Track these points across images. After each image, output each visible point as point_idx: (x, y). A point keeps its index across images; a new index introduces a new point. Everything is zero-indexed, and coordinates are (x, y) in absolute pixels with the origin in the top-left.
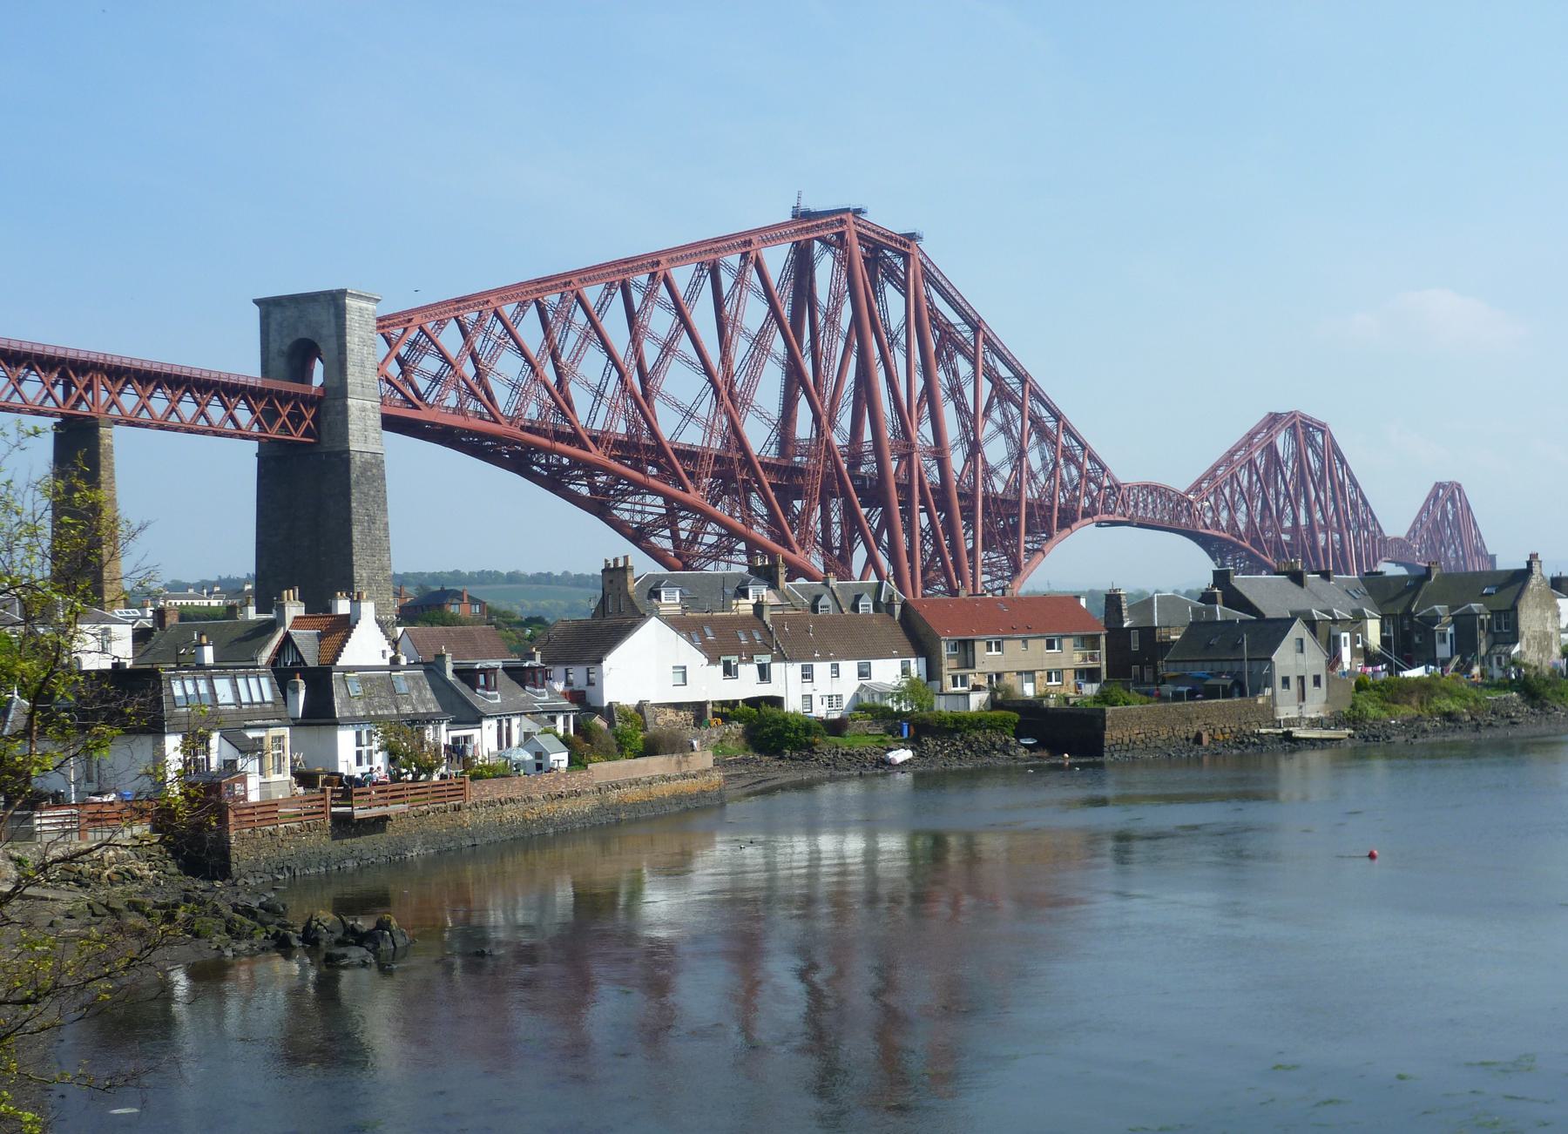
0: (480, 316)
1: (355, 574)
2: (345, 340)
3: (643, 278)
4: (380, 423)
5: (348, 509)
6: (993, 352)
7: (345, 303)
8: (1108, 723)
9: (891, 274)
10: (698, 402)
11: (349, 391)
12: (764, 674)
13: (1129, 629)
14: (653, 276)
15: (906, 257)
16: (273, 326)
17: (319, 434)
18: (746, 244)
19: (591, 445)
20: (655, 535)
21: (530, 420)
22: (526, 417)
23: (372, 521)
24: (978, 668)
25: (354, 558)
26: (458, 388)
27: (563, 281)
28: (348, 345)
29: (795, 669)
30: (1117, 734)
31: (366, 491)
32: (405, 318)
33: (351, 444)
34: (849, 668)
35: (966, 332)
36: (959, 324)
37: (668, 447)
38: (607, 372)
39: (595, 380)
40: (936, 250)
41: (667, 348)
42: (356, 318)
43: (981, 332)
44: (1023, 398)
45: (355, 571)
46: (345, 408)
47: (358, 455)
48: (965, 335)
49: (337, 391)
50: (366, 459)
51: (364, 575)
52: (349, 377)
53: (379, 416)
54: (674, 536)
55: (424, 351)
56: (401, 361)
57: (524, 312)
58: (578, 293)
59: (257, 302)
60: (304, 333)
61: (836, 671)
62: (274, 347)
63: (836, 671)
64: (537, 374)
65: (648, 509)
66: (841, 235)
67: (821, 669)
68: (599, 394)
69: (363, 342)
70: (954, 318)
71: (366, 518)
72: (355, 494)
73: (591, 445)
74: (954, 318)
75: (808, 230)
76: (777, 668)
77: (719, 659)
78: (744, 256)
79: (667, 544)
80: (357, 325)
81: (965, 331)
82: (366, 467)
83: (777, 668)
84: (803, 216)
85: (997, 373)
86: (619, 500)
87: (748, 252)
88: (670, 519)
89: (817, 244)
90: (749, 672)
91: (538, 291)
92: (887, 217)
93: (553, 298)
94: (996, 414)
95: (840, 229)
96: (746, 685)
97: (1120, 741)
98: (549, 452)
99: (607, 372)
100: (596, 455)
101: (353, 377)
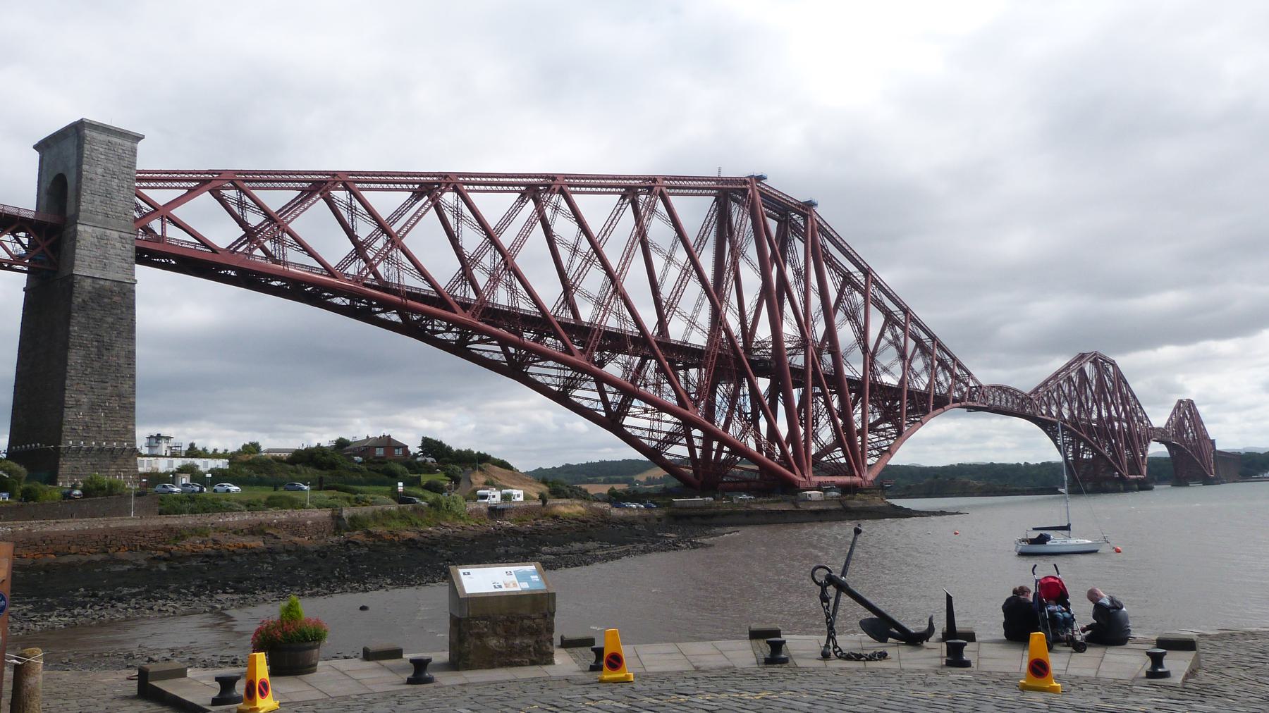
1: (66, 399)
4: (133, 254)
5: (68, 333)
6: (879, 289)
23: (104, 347)
25: (68, 382)
31: (98, 316)
36: (855, 272)
37: (554, 320)
42: (101, 149)
43: (870, 276)
44: (906, 323)
45: (67, 395)
47: (89, 281)
70: (852, 268)
71: (95, 343)
72: (78, 318)
74: (852, 268)
80: (103, 157)
85: (883, 304)
94: (888, 334)
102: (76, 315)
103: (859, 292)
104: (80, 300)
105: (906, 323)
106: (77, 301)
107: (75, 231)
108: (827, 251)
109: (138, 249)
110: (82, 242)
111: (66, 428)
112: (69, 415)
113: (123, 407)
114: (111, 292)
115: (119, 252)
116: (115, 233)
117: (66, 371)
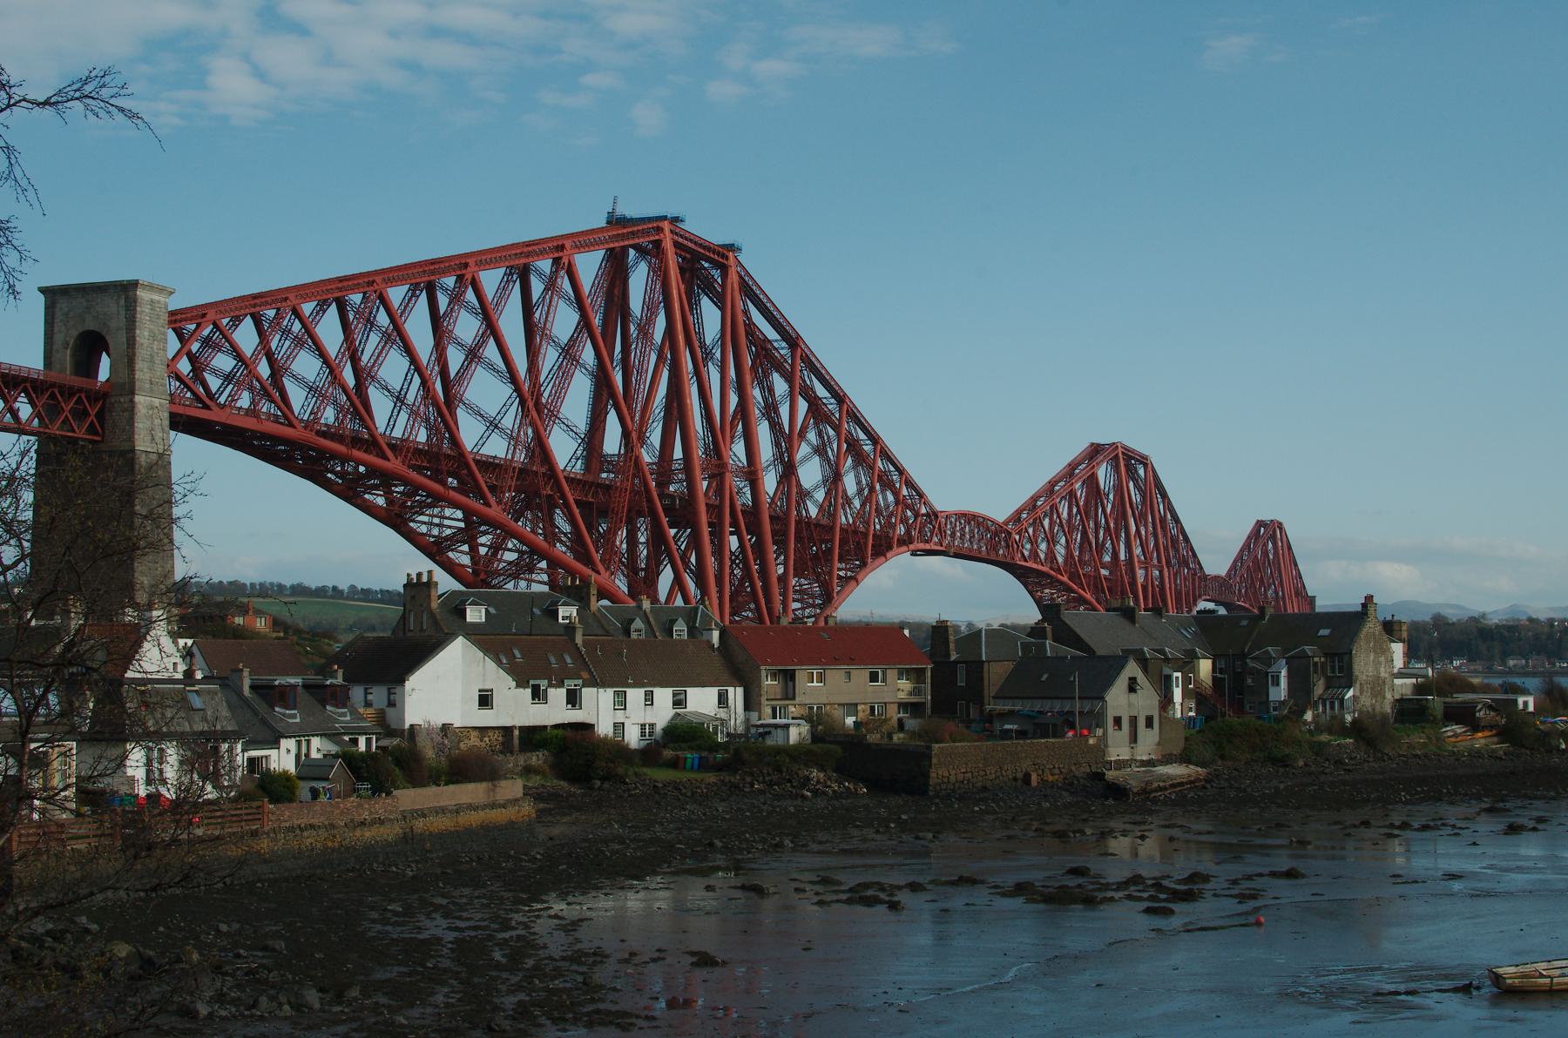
0: (277, 314)
2: (135, 333)
3: (450, 281)
4: (167, 423)
6: (811, 370)
7: (136, 295)
8: (934, 761)
9: (708, 288)
10: (503, 411)
11: (137, 387)
12: (573, 699)
13: (956, 662)
14: (460, 278)
15: (724, 269)
16: (59, 315)
17: (103, 432)
18: (560, 249)
19: (389, 453)
20: (452, 550)
21: (326, 425)
22: (322, 421)
24: (798, 700)
26: (251, 389)
27: (366, 280)
28: (138, 339)
29: (606, 696)
30: (942, 772)
32: (199, 314)
33: (137, 443)
34: (663, 696)
35: (783, 349)
36: (776, 341)
38: (409, 377)
39: (396, 384)
40: (756, 263)
41: (473, 355)
42: (147, 311)
43: (799, 349)
44: (840, 420)
46: (131, 409)
48: (782, 352)
49: (125, 387)
52: (137, 372)
53: (166, 415)
54: (473, 550)
55: (218, 348)
56: (192, 358)
57: (324, 312)
58: (381, 293)
59: (43, 290)
60: (91, 325)
61: (649, 699)
62: (59, 338)
63: (649, 699)
64: (336, 378)
65: (446, 522)
66: (658, 244)
67: (635, 695)
68: (399, 399)
69: (153, 337)
70: (771, 334)
73: (389, 453)
74: (771, 334)
75: (623, 237)
76: (588, 693)
77: (528, 682)
78: (556, 261)
79: (466, 560)
80: (148, 318)
81: (782, 348)
83: (588, 693)
84: (615, 221)
86: (416, 512)
87: (560, 258)
88: (468, 535)
89: (632, 252)
90: (558, 695)
91: (340, 289)
92: (707, 228)
93: (356, 298)
94: (812, 436)
95: (657, 237)
96: (554, 711)
97: (946, 780)
98: (344, 460)
99: (409, 377)
100: (394, 464)
101: (142, 372)
103: (782, 375)
105: (840, 420)
107: (132, 401)
108: (750, 319)
109: (172, 416)
116: (157, 400)
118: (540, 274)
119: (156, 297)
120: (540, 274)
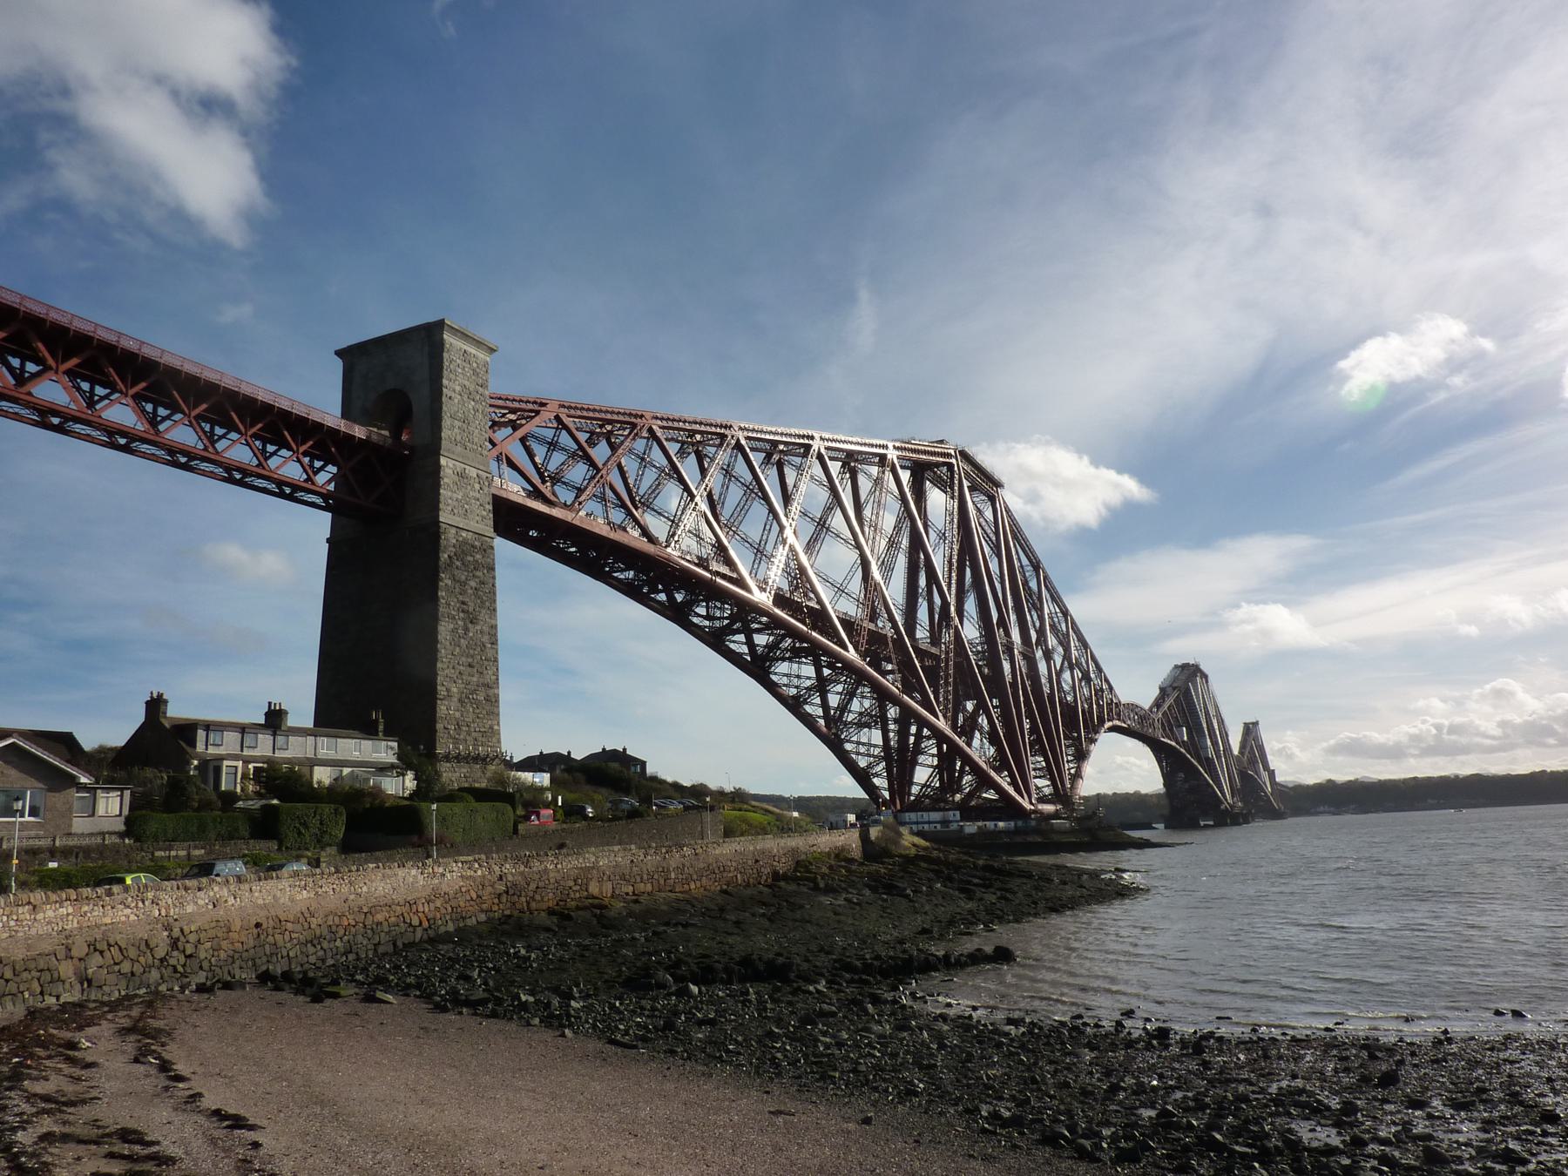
1: (439, 688)
10: (849, 577)
38: (768, 527)
47: (453, 531)
50: (464, 539)
51: (455, 690)
54: (825, 705)
59: (339, 353)
71: (462, 615)
72: (445, 580)
82: (464, 548)
88: (822, 686)
99: (768, 527)
102: (443, 575)
104: (446, 556)
106: (444, 556)
110: (446, 480)
111: (439, 726)
112: (442, 709)
113: (487, 699)
114: (473, 546)
115: (478, 495)
117: (436, 651)
118: (869, 476)
119: (472, 350)
120: (869, 476)
